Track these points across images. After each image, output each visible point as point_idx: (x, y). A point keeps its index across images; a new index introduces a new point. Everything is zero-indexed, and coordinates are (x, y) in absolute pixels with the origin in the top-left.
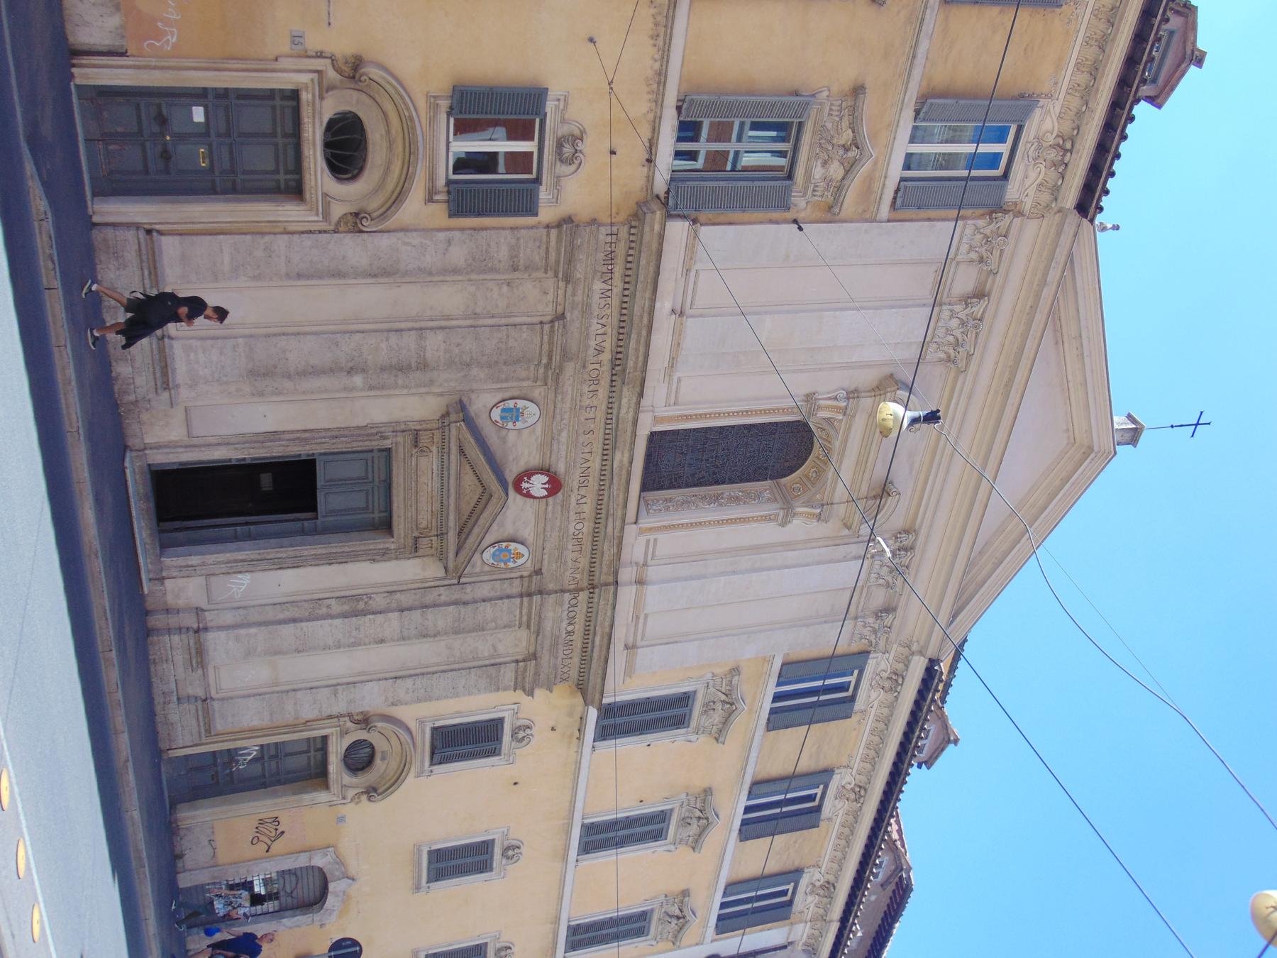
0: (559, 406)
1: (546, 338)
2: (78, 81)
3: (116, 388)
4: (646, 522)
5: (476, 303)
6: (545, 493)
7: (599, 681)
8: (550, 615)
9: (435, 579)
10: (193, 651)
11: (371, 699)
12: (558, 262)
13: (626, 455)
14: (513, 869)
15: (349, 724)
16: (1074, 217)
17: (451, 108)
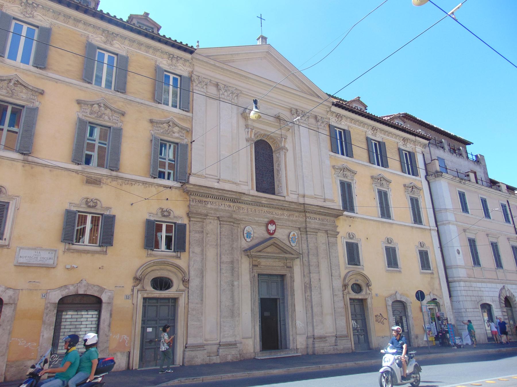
1: (225, 223)
2: (137, 367)
4: (285, 194)
6: (274, 225)
7: (335, 211)
8: (313, 225)
9: (300, 262)
10: (321, 340)
11: (338, 284)
12: (201, 218)
13: (263, 199)
14: (395, 240)
15: (346, 291)
16: (194, 55)
17: (151, 250)
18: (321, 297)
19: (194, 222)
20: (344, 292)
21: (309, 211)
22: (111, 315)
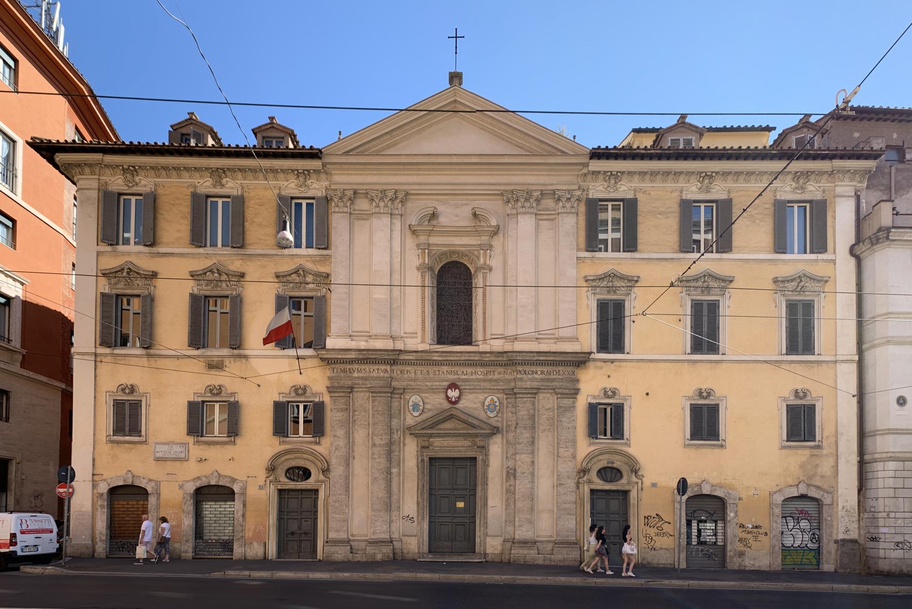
0: (413, 387)
1: (379, 395)
2: (274, 557)
3: (386, 559)
5: (363, 424)
6: (457, 390)
7: (570, 355)
9: (502, 438)
10: (525, 545)
12: (344, 392)
13: (434, 354)
17: (284, 436)
18: (532, 488)
19: (335, 398)
20: (581, 480)
21: (520, 361)
22: (244, 506)
